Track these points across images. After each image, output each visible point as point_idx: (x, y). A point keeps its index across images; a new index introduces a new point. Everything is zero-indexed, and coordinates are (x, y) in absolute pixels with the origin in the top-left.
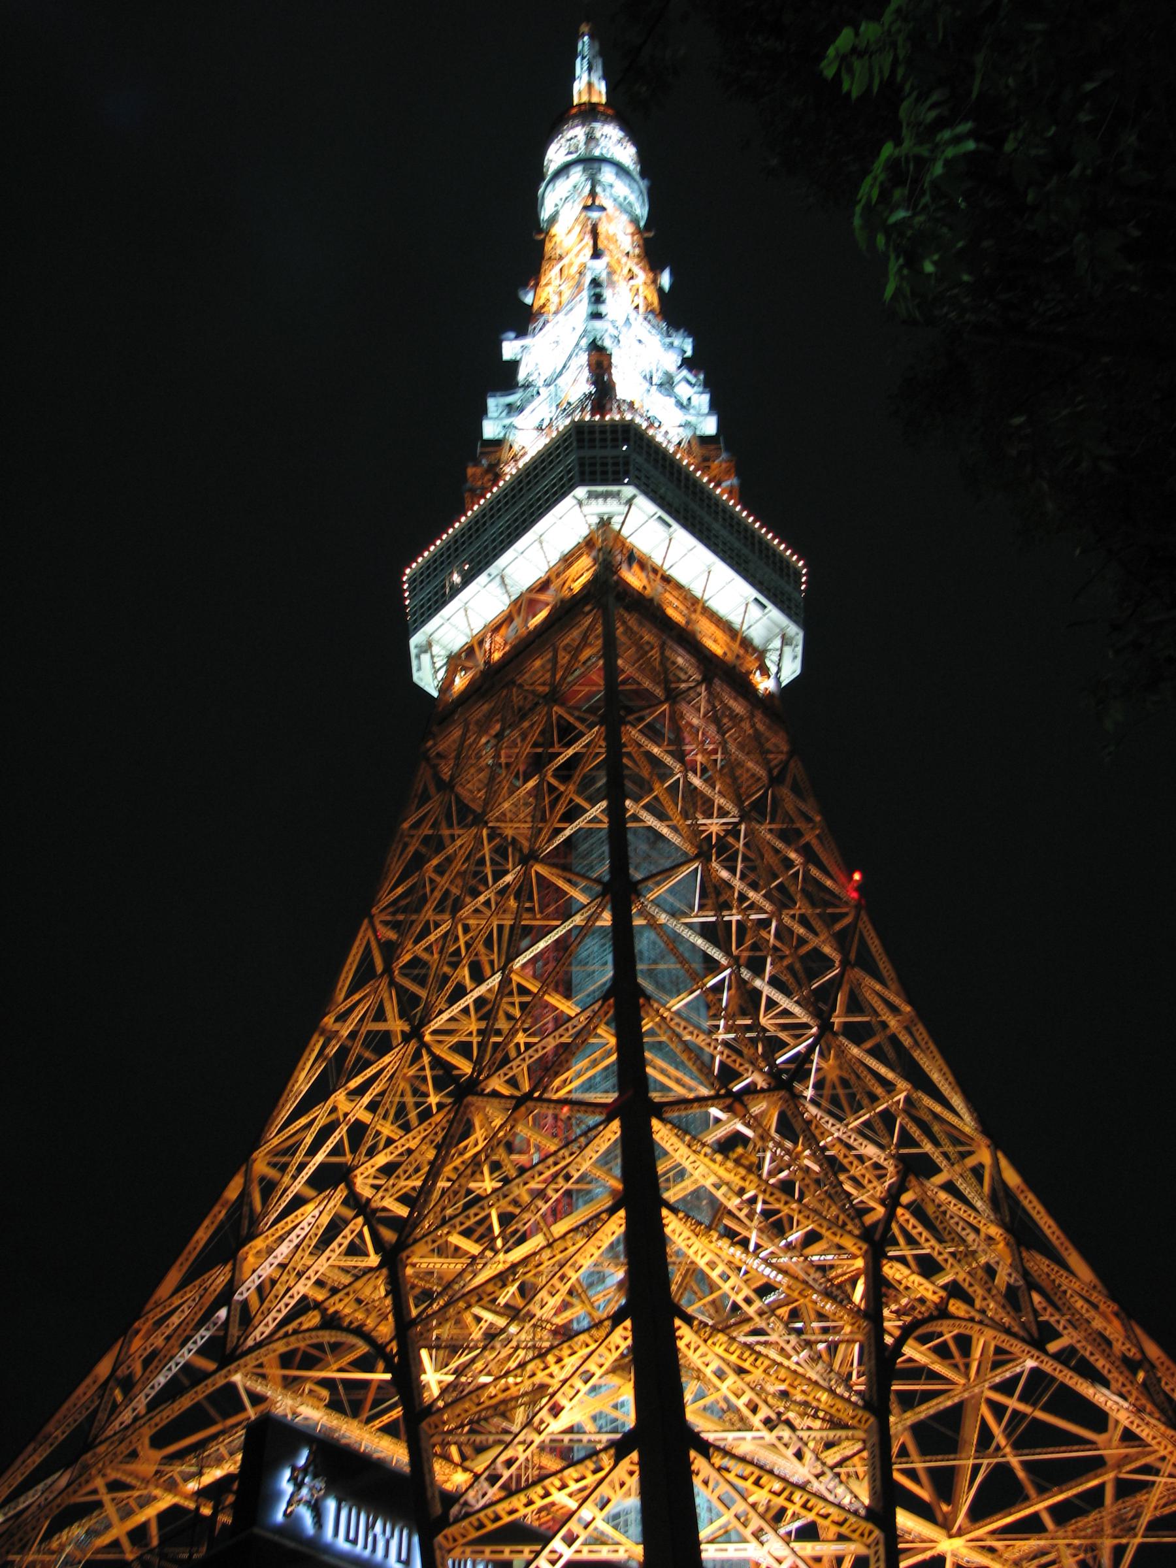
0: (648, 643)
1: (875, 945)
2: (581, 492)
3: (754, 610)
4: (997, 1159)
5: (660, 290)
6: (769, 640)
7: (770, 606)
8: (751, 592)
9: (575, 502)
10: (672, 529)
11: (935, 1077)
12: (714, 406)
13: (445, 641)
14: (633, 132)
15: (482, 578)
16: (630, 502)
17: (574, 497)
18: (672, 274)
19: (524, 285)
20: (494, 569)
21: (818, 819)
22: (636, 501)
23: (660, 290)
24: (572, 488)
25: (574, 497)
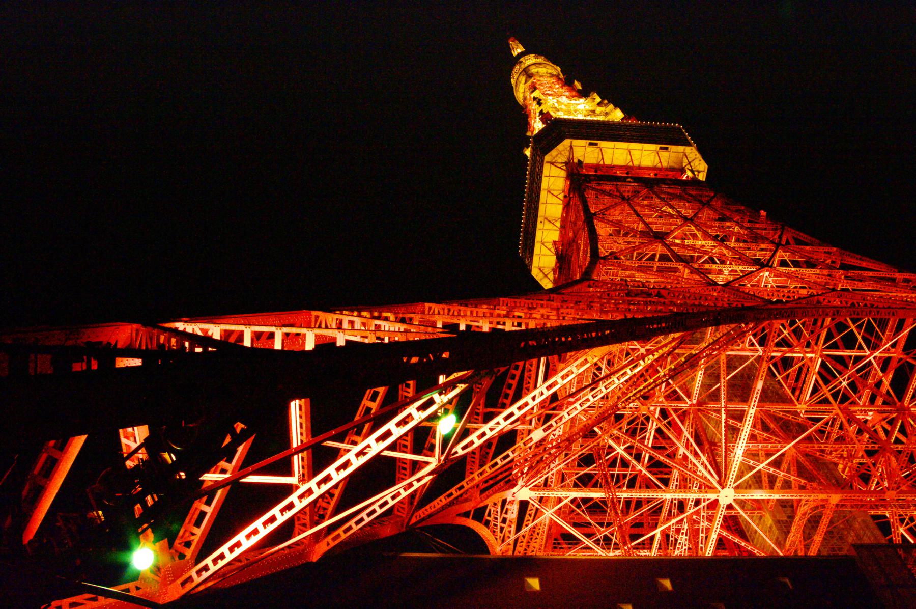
0: (610, 190)
1: (803, 236)
2: (547, 158)
3: (664, 154)
6: (682, 163)
7: (669, 146)
8: (654, 147)
9: (549, 165)
10: (599, 146)
11: (864, 264)
12: (616, 106)
13: (546, 265)
14: (538, 53)
15: (539, 226)
16: (571, 147)
17: (547, 162)
18: (578, 81)
19: (526, 131)
20: (539, 219)
21: (743, 208)
22: (573, 144)
23: (578, 91)
24: (543, 161)
25: (547, 162)
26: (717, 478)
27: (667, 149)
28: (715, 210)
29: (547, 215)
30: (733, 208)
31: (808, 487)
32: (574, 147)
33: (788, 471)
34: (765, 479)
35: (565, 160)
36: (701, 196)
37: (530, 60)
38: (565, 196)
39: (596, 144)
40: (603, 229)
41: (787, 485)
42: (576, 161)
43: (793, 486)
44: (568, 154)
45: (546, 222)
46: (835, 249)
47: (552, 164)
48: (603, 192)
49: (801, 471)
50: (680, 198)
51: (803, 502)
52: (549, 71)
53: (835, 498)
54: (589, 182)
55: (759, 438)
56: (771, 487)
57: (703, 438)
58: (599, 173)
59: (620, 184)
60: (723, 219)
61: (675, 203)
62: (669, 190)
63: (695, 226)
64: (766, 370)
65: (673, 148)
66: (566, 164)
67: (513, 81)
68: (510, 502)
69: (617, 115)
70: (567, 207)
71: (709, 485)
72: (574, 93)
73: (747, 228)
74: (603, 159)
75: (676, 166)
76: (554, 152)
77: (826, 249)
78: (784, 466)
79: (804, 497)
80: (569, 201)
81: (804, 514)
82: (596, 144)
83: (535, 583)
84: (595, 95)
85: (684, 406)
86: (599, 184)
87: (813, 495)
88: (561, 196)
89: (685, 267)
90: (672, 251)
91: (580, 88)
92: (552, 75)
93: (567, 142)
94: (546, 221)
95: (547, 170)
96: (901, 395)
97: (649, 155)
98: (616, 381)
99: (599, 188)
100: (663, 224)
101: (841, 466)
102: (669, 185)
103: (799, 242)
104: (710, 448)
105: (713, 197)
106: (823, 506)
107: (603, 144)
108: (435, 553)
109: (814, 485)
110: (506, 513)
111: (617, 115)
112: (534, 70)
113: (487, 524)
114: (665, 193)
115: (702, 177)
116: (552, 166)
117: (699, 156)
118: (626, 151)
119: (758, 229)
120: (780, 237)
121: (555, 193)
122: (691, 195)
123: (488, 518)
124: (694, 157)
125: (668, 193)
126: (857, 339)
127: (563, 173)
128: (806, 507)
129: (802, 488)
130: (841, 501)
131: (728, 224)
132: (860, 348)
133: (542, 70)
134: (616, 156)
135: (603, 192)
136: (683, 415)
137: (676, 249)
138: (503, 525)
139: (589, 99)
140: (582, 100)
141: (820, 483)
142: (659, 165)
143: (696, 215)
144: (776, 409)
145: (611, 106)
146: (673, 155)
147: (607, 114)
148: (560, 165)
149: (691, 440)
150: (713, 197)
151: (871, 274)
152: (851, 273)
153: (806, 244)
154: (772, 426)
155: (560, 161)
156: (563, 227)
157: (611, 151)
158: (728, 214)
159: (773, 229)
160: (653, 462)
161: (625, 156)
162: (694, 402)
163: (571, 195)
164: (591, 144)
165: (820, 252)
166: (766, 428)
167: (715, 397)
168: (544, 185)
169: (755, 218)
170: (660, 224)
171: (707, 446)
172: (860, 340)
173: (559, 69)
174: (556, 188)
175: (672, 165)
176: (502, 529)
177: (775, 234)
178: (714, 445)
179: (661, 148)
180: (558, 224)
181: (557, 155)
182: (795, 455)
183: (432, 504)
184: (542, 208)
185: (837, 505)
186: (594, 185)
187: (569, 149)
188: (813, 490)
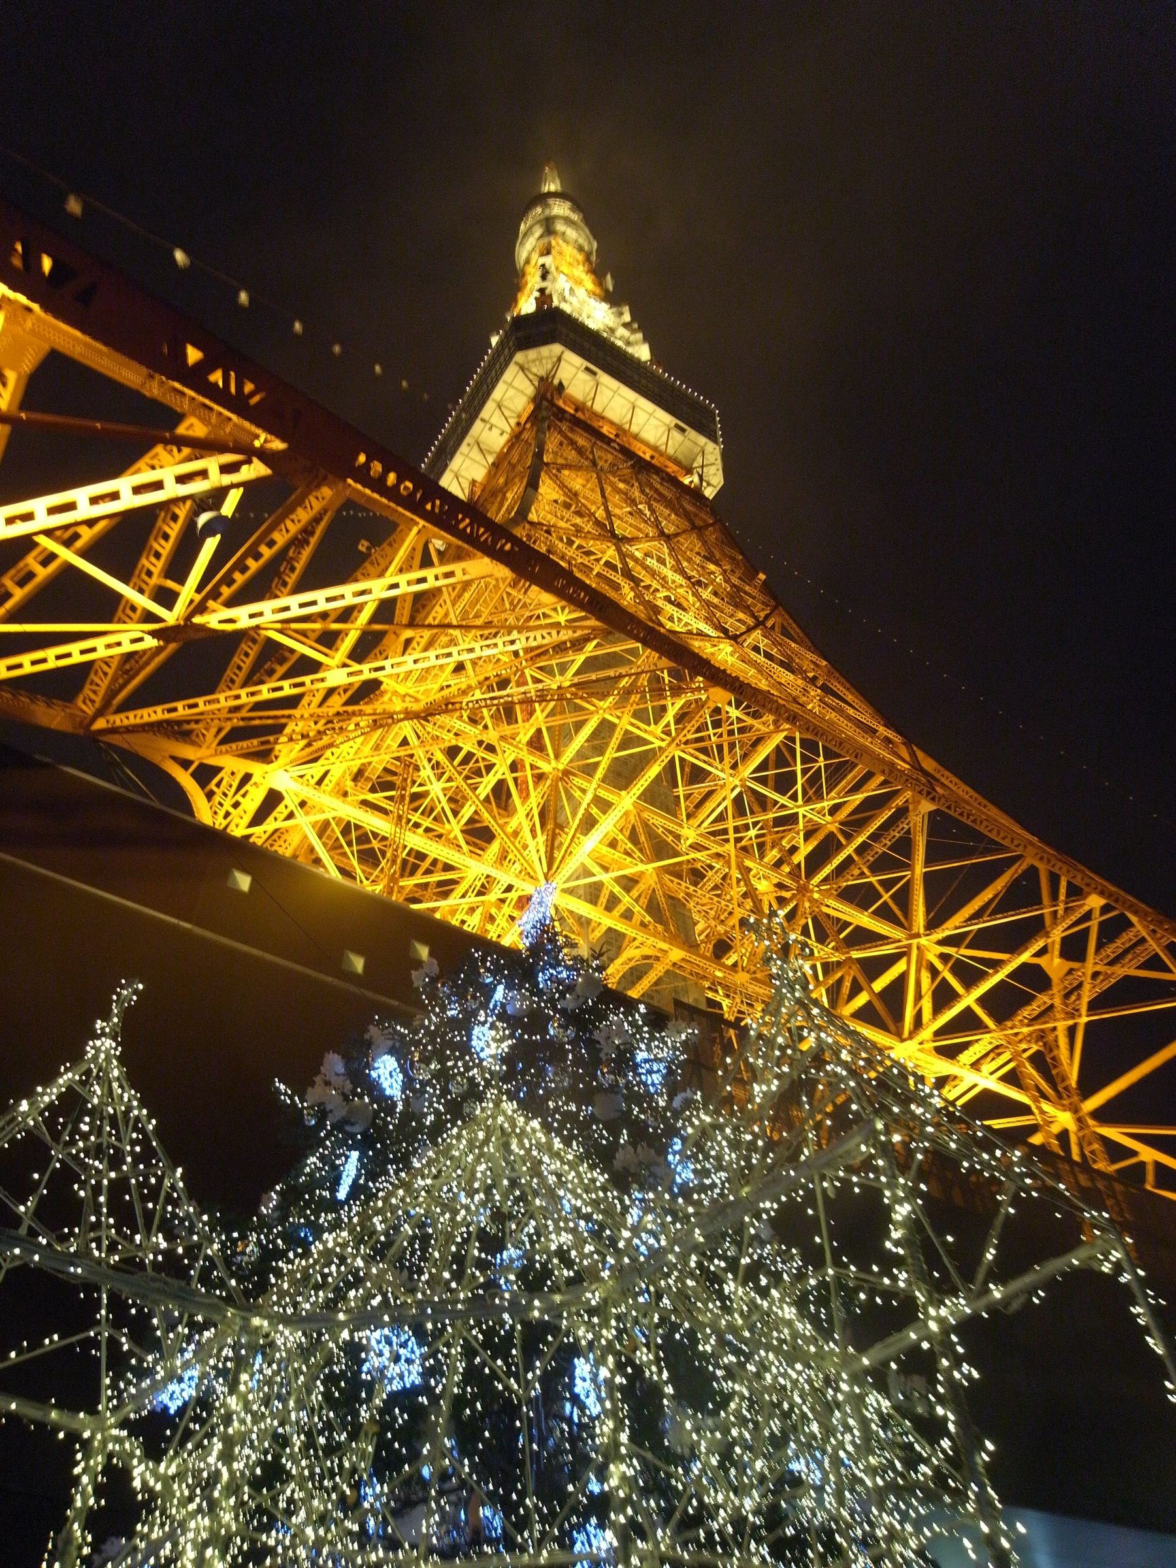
1: (794, 629)
2: (519, 357)
3: (676, 435)
4: (914, 752)
5: (607, 291)
6: (694, 460)
8: (668, 419)
9: (517, 368)
12: (646, 339)
14: (577, 206)
15: (463, 448)
16: (559, 359)
17: (517, 363)
20: (468, 439)
23: (607, 291)
24: (511, 357)
25: (517, 363)
26: (546, 870)
27: (683, 430)
28: (705, 543)
29: (481, 439)
30: (728, 550)
31: (651, 927)
32: (562, 363)
33: (637, 900)
34: (605, 894)
35: (542, 373)
36: (696, 515)
37: (560, 209)
38: (518, 424)
39: (594, 374)
40: (548, 490)
41: (628, 915)
42: (556, 382)
43: (634, 920)
44: (550, 366)
45: (476, 448)
46: (825, 663)
47: (522, 368)
48: (572, 443)
49: (652, 908)
50: (669, 504)
51: (636, 943)
52: (581, 241)
53: (676, 954)
54: (561, 421)
55: (619, 848)
56: (609, 908)
57: (551, 815)
58: (579, 415)
59: (598, 443)
60: (710, 558)
61: (660, 508)
62: (658, 486)
63: (671, 549)
64: (666, 761)
65: (692, 434)
66: (541, 379)
67: (522, 227)
68: (255, 784)
69: (643, 352)
70: (516, 438)
71: (532, 873)
72: (598, 291)
73: (733, 586)
74: (594, 399)
75: (684, 462)
76: (532, 354)
77: (814, 658)
78: (635, 893)
79: (641, 937)
80: (521, 433)
81: (630, 960)
82: (594, 374)
83: (244, 882)
84: (626, 310)
85: (545, 767)
86: (572, 430)
87: (652, 939)
88: (513, 422)
89: (632, 589)
90: (625, 564)
91: (611, 288)
92: (580, 249)
93: (557, 348)
94: (476, 446)
95: (511, 373)
96: (810, 873)
97: (657, 427)
98: (478, 649)
99: (570, 435)
100: (631, 525)
101: (699, 928)
102: (662, 479)
103: (785, 632)
104: (554, 831)
105: (711, 525)
106: (657, 959)
107: (605, 379)
108: (115, 784)
109: (660, 928)
110: (244, 796)
111: (643, 352)
112: (560, 227)
113: (210, 795)
114: (652, 487)
115: (709, 493)
116: (521, 373)
117: (719, 462)
118: (630, 405)
119: (746, 593)
120: (767, 617)
121: (507, 413)
122: (684, 509)
123: (215, 789)
124: (712, 461)
125: (656, 490)
126: (796, 783)
127: (530, 391)
128: (637, 951)
129: (643, 925)
130: (683, 959)
131: (712, 567)
132: (794, 797)
133: (571, 233)
134: (613, 404)
135: (572, 443)
136: (540, 777)
137: (631, 564)
138: (231, 810)
139: (614, 310)
140: (605, 306)
141: (667, 930)
142: (663, 447)
143: (677, 535)
144: (658, 820)
145: (639, 336)
146: (687, 443)
147: (628, 343)
148: (531, 376)
149: (536, 812)
150: (711, 525)
151: (851, 712)
152: (829, 699)
153: (795, 642)
154: (642, 838)
155: (535, 370)
156: (496, 465)
157: (610, 394)
158: (718, 556)
159: (763, 603)
160: (470, 827)
161: (624, 411)
162: (561, 767)
163: (528, 426)
164: (587, 369)
165: (808, 659)
166: (633, 838)
167: (590, 770)
168: (497, 394)
169: (749, 577)
170: (626, 522)
171: (550, 826)
172: (799, 786)
173: (595, 245)
174: (512, 407)
175: (680, 457)
176: (227, 814)
177: (763, 610)
178: (561, 827)
179: (677, 426)
180: (491, 459)
181: (534, 361)
182: (654, 885)
183: (139, 712)
184: (478, 426)
185: (674, 964)
186: (564, 427)
187: (555, 359)
188: (655, 934)
